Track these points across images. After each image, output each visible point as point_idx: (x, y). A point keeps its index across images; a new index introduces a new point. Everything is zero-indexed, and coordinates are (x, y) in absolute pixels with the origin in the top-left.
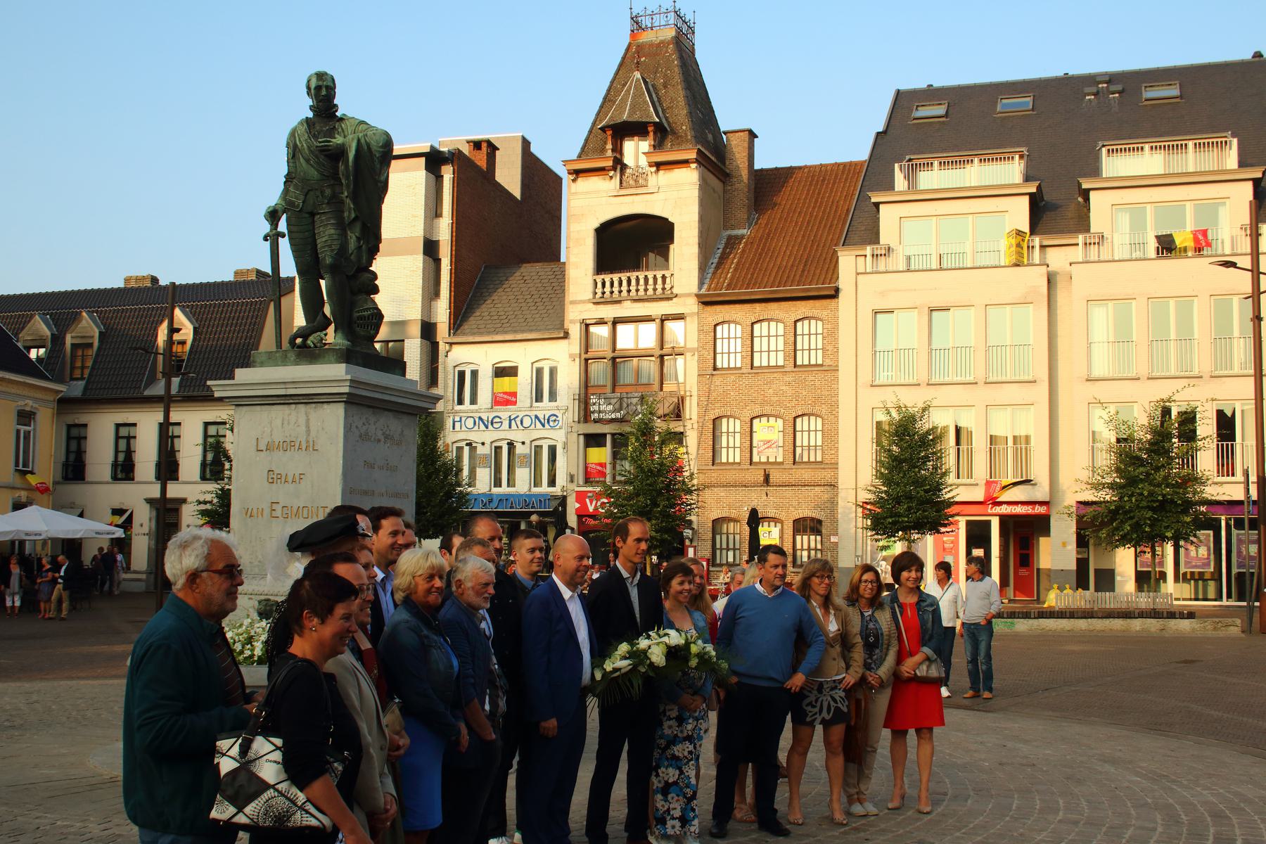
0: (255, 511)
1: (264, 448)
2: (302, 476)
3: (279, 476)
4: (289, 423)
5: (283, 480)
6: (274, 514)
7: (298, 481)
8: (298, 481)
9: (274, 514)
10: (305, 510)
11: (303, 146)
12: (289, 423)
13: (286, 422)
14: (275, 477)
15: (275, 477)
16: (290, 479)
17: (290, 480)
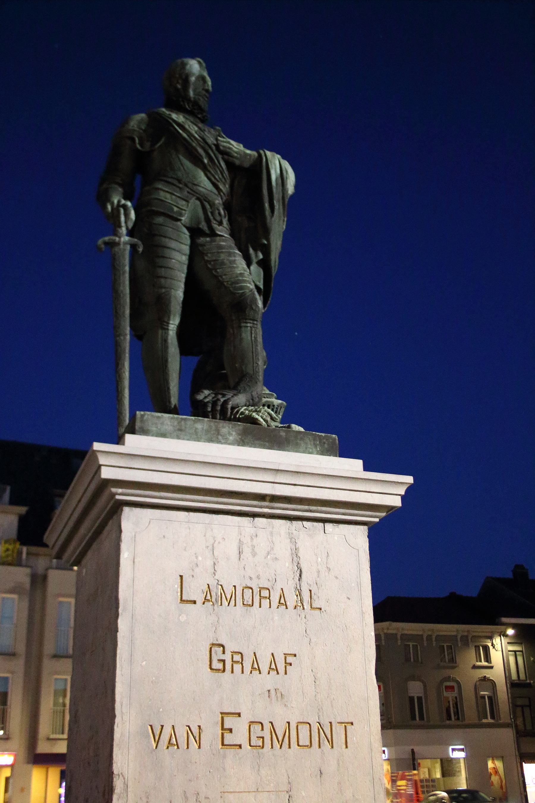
0: (182, 733)
1: (200, 599)
2: (290, 659)
4: (254, 554)
6: (229, 739)
7: (281, 669)
8: (281, 669)
9: (229, 739)
10: (304, 731)
11: (192, 126)
12: (254, 554)
13: (247, 550)
14: (227, 657)
15: (227, 657)
16: (264, 666)
17: (264, 666)
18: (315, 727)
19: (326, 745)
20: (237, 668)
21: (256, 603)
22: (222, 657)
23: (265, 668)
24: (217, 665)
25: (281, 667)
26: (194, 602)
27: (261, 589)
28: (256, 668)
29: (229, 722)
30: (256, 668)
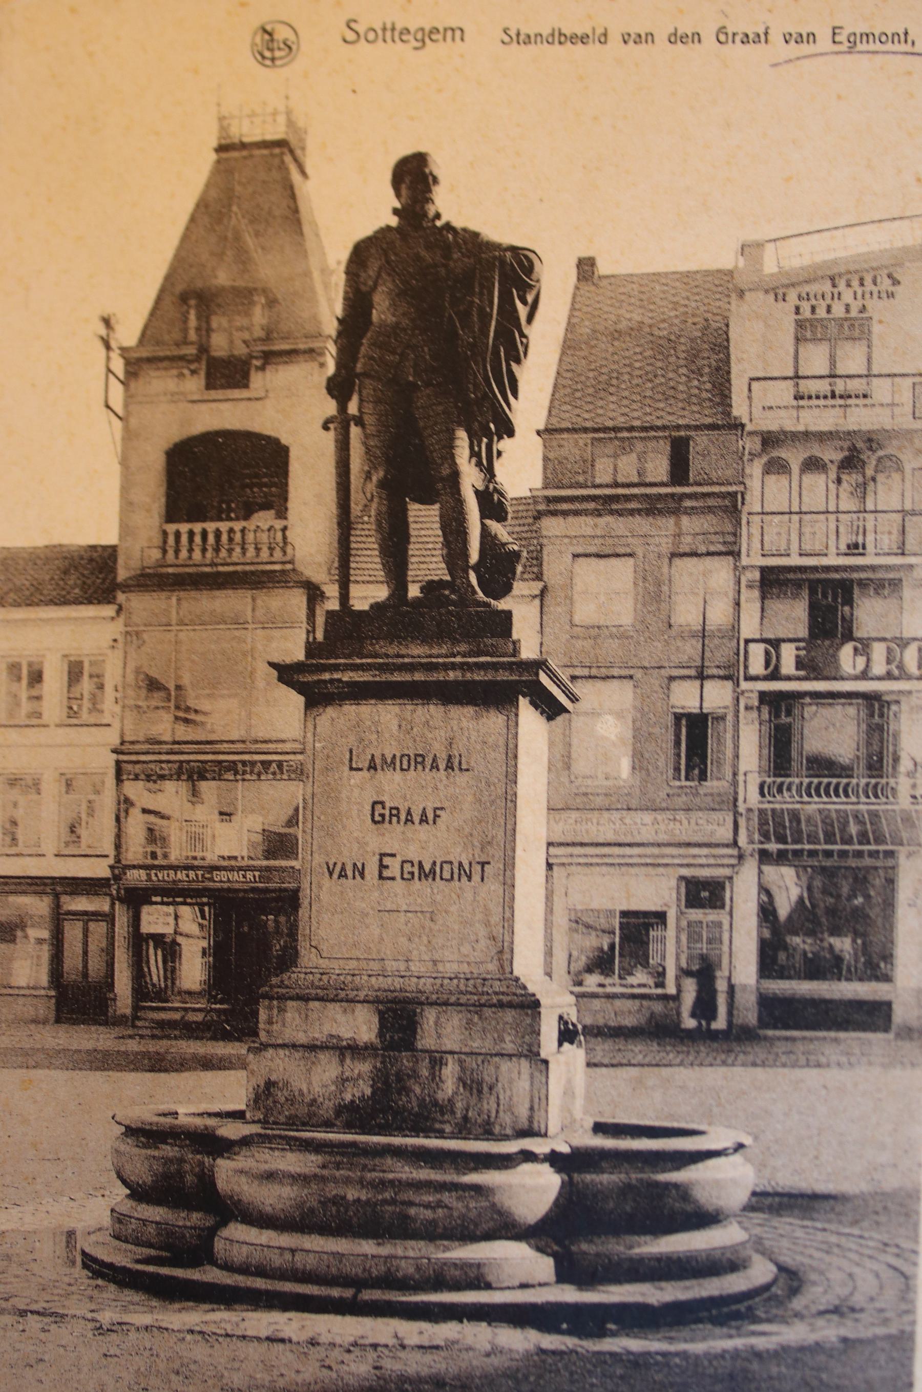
2: (438, 812)
3: (394, 812)
5: (403, 817)
6: (386, 873)
7: (431, 822)
14: (387, 813)
16: (417, 819)
18: (456, 865)
19: (464, 879)
20: (395, 819)
21: (412, 768)
22: (382, 811)
23: (417, 819)
24: (377, 818)
25: (430, 816)
26: (360, 769)
27: (416, 755)
28: (409, 820)
29: (387, 861)
30: (409, 820)
